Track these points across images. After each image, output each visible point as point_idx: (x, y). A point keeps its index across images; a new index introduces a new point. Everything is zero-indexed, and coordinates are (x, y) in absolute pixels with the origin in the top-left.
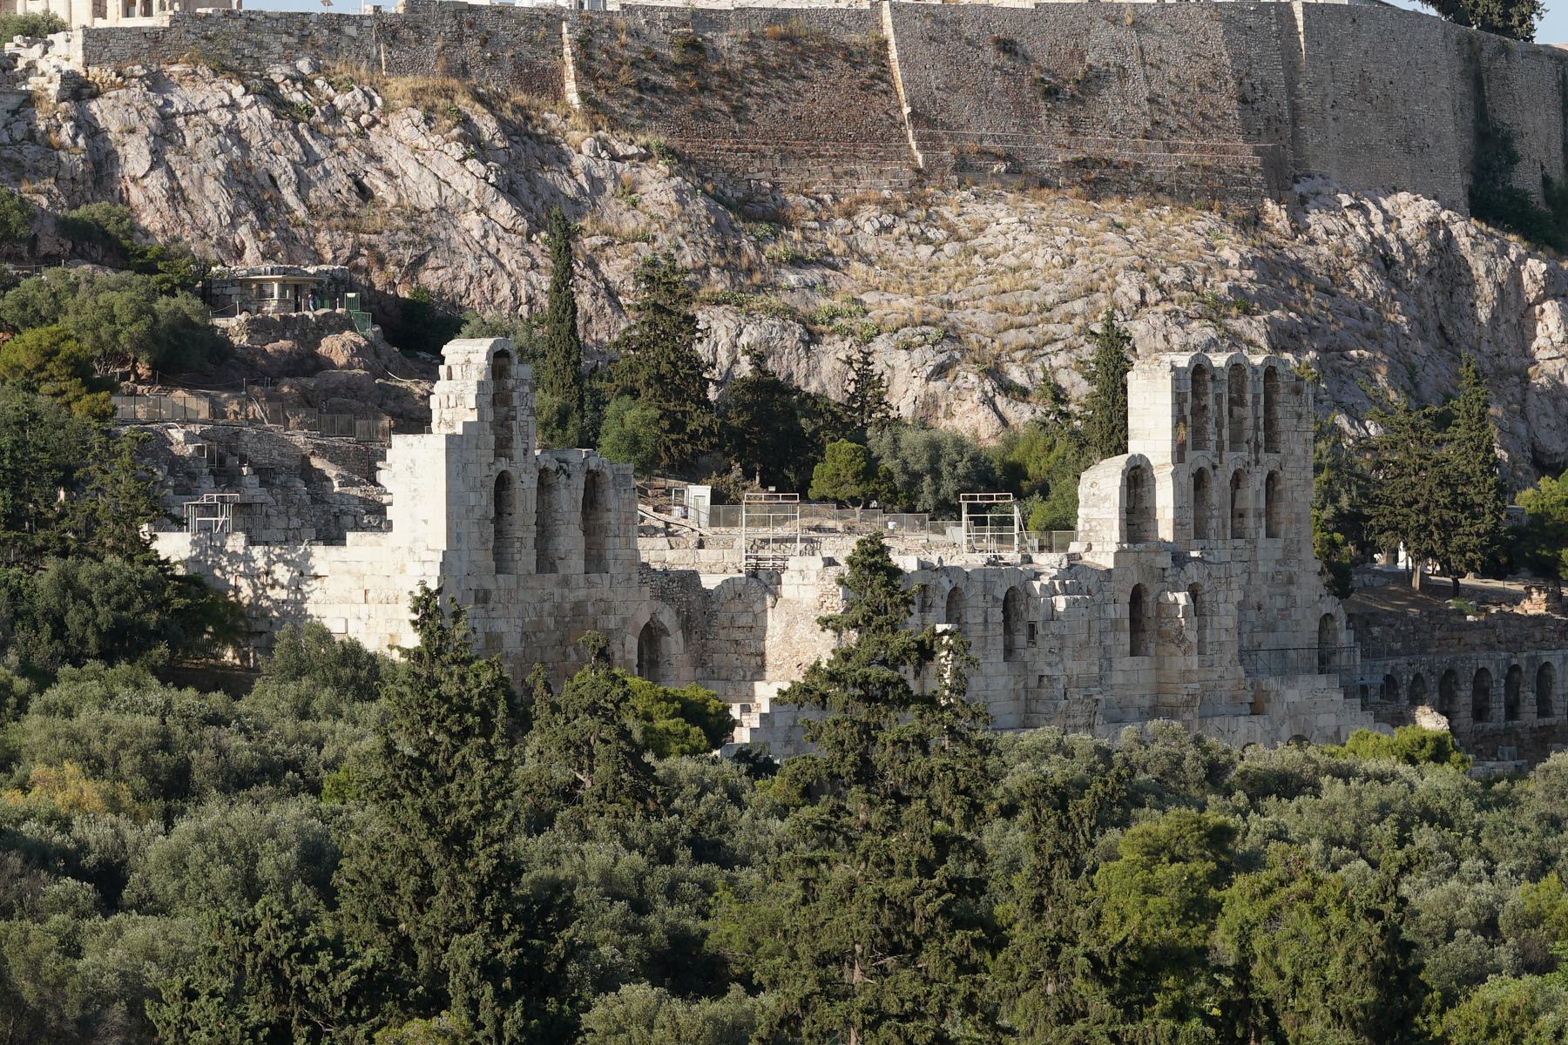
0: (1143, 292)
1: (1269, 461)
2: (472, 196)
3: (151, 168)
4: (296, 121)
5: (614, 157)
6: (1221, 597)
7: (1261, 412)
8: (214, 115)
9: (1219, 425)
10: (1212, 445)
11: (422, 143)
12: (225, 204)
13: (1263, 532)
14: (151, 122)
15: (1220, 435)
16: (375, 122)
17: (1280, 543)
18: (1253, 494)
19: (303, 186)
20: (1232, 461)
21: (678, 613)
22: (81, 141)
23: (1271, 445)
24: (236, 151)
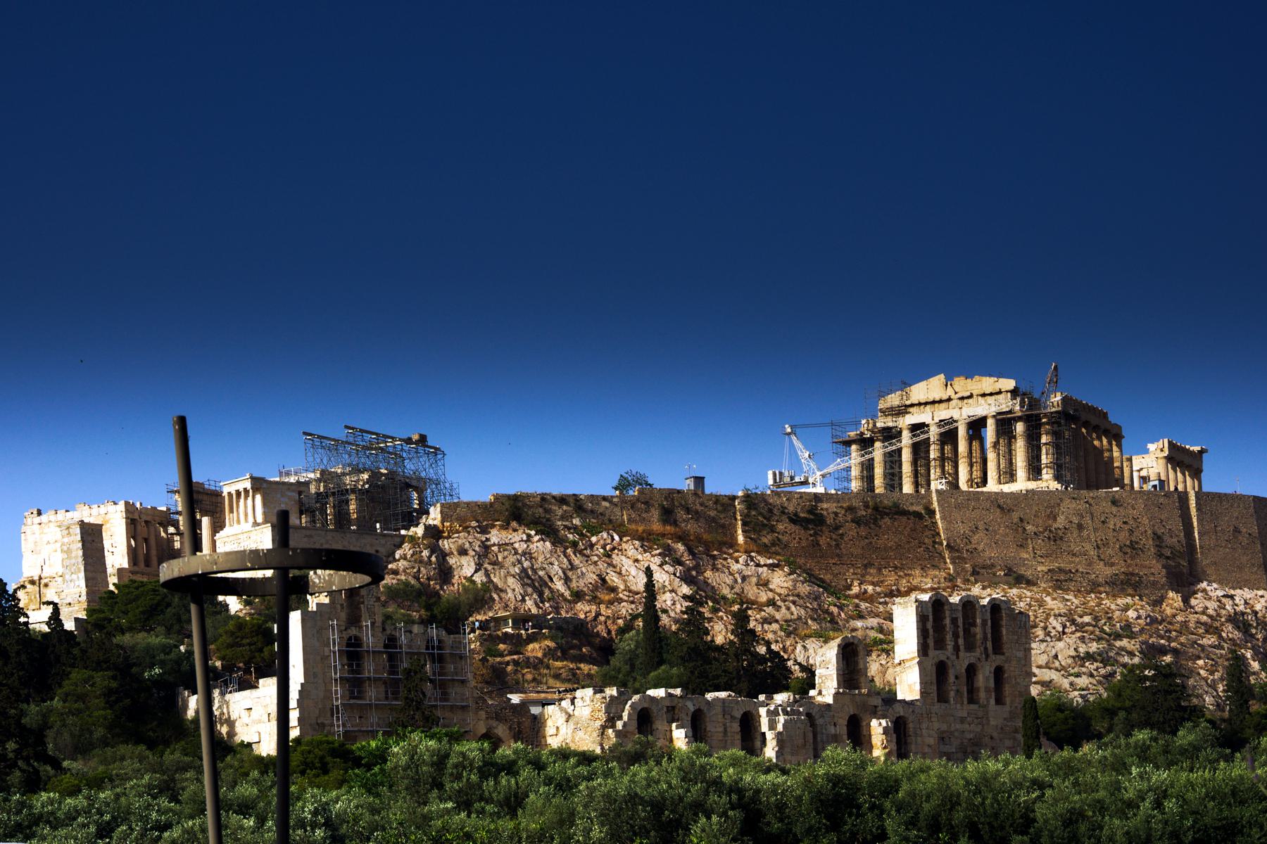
0: (1064, 627)
1: (998, 660)
2: (667, 583)
3: (476, 571)
4: (566, 548)
5: (758, 565)
6: (924, 726)
7: (989, 630)
8: (516, 545)
9: (956, 636)
10: (950, 647)
11: (640, 557)
12: (519, 590)
13: (993, 701)
14: (477, 549)
15: (956, 642)
16: (614, 548)
17: (1007, 708)
18: (984, 678)
19: (567, 580)
20: (966, 659)
21: (510, 728)
22: (433, 559)
23: (998, 648)
24: (527, 564)
